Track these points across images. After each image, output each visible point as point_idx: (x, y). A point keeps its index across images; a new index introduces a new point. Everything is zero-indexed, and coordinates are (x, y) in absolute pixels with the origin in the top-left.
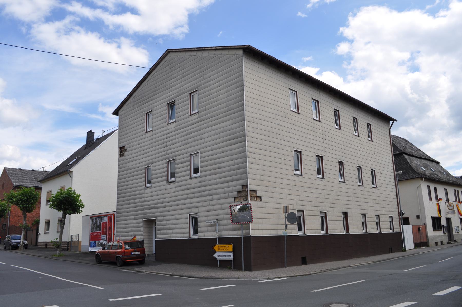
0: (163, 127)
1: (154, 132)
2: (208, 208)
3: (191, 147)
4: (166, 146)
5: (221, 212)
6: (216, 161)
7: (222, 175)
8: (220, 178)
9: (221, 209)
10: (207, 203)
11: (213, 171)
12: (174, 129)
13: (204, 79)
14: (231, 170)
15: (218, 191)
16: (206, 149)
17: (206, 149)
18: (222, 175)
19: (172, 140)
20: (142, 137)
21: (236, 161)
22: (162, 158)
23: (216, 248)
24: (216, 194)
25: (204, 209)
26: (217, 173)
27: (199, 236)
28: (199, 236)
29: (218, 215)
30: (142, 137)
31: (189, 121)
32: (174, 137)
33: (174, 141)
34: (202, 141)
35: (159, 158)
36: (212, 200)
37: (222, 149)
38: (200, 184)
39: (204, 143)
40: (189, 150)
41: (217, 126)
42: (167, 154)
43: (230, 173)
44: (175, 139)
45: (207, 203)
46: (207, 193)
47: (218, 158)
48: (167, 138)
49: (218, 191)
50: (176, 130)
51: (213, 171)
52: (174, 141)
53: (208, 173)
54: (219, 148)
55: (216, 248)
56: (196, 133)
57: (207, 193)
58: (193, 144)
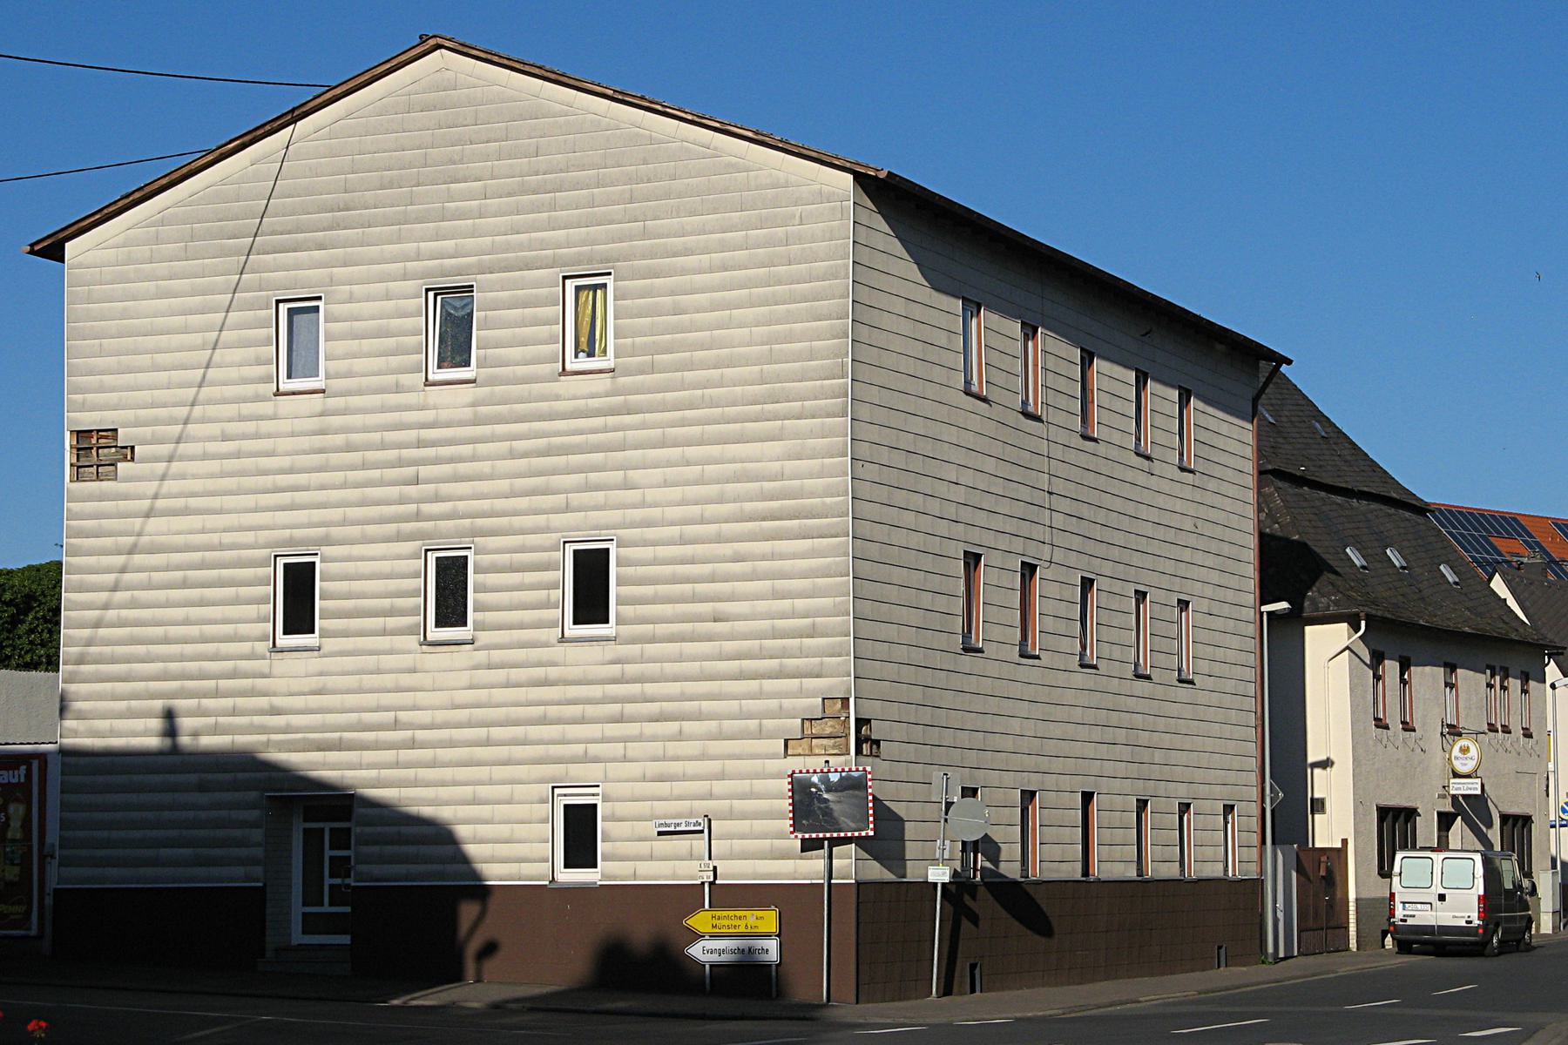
0: (398, 389)
1: (332, 402)
2: (653, 768)
3: (568, 509)
4: (417, 481)
5: (718, 787)
6: (701, 588)
7: (729, 646)
8: (722, 657)
9: (721, 776)
10: (656, 748)
11: (687, 627)
12: (467, 413)
13: (645, 235)
14: (776, 634)
15: (706, 705)
16: (650, 533)
17: (650, 533)
18: (729, 646)
19: (451, 460)
20: (247, 409)
21: (800, 603)
22: (391, 528)
23: (700, 921)
24: (698, 717)
25: (634, 769)
26: (709, 638)
27: (604, 877)
28: (604, 877)
29: (710, 796)
30: (247, 409)
31: (557, 398)
32: (466, 449)
33: (463, 468)
34: (632, 495)
35: (372, 529)
36: (680, 737)
37: (736, 545)
38: (615, 670)
39: (643, 504)
40: (558, 520)
41: (715, 450)
42: (418, 517)
43: (768, 643)
44: (474, 458)
45: (656, 748)
46: (654, 708)
47: (712, 579)
48: (420, 444)
49: (706, 705)
50: (476, 422)
51: (687, 627)
52: (463, 468)
53: (662, 629)
54: (719, 539)
55: (700, 921)
56: (598, 457)
57: (654, 708)
58: (576, 498)
